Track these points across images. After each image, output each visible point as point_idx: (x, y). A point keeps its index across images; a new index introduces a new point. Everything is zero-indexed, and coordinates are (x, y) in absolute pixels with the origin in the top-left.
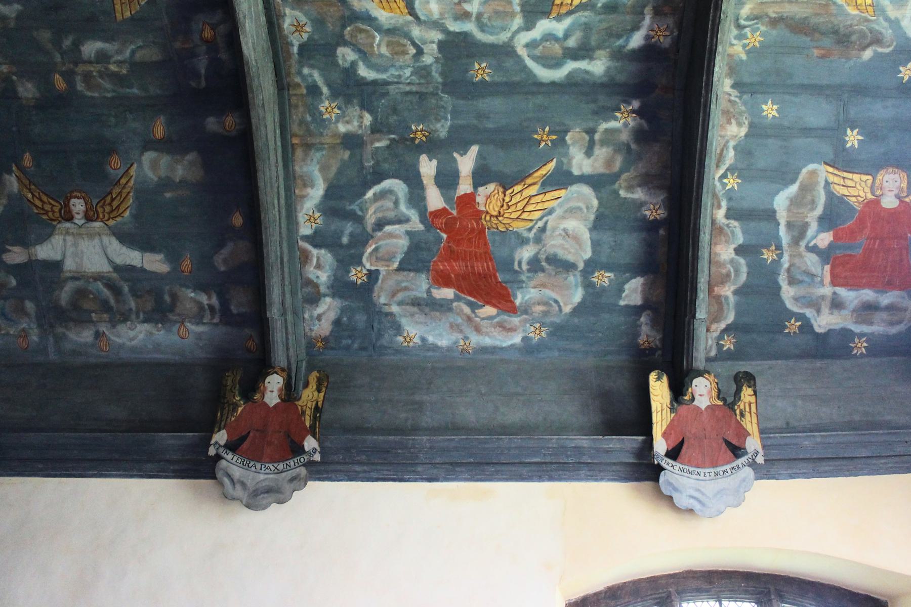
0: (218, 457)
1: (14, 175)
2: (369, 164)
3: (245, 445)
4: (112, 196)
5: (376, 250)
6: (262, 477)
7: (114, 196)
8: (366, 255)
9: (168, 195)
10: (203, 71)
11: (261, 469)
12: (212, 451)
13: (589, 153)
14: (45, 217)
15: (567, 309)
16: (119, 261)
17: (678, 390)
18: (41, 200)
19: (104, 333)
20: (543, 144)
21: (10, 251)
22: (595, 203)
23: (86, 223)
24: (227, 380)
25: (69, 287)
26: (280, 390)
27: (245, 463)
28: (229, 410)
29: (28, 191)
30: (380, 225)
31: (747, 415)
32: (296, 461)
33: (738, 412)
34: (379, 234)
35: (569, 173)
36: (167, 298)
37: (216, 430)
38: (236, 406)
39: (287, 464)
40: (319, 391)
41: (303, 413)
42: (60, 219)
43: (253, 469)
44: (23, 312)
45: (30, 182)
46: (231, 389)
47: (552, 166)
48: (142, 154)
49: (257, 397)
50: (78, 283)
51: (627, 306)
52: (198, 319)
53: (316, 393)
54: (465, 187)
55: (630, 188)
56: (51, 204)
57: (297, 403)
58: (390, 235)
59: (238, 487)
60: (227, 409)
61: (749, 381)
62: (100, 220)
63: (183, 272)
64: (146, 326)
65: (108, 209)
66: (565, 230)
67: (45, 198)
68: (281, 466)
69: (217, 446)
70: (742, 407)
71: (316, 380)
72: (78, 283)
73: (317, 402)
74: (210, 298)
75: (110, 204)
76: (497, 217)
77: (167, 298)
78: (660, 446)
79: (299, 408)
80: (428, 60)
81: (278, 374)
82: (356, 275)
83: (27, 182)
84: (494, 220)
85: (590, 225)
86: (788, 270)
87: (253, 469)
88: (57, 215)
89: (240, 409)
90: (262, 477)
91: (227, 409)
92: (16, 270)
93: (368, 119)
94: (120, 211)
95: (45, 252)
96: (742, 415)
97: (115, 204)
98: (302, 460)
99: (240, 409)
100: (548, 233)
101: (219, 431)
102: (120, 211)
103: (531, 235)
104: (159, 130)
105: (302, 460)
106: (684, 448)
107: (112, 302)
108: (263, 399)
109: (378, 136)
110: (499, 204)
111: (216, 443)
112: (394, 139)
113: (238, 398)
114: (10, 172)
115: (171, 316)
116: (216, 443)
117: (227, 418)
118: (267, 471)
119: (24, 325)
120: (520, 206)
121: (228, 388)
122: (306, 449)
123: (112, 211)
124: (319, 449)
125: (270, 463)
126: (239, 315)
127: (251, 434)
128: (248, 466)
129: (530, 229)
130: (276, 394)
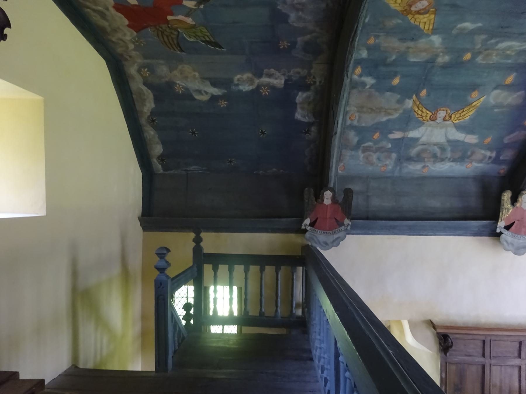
0: (501, 233)
1: (412, 100)
3: (513, 228)
4: (464, 110)
6: (521, 241)
7: (465, 110)
9: (496, 110)
14: (421, 119)
16: (451, 138)
18: (422, 111)
19: (428, 166)
21: (394, 133)
23: (442, 122)
24: (504, 197)
25: (419, 148)
28: (505, 212)
29: (417, 107)
36: (469, 153)
37: (500, 221)
38: (508, 209)
42: (429, 120)
44: (389, 157)
45: (420, 103)
49: (518, 205)
50: (424, 147)
52: (481, 161)
56: (426, 113)
59: (510, 246)
60: (505, 211)
62: (451, 120)
63: (484, 143)
64: (452, 164)
65: (458, 115)
67: (424, 110)
69: (500, 228)
72: (424, 147)
74: (492, 153)
77: (469, 153)
83: (418, 103)
88: (428, 118)
89: (510, 211)
90: (521, 241)
91: (505, 211)
92: (397, 143)
95: (412, 134)
97: (464, 113)
99: (510, 211)
101: (501, 221)
104: (510, 79)
107: (439, 154)
108: (521, 206)
111: (500, 227)
113: (509, 206)
114: (410, 98)
115: (467, 160)
117: (505, 215)
118: (524, 239)
119: (387, 163)
121: (505, 201)
123: (460, 116)
125: (524, 235)
126: (502, 160)
128: (515, 237)
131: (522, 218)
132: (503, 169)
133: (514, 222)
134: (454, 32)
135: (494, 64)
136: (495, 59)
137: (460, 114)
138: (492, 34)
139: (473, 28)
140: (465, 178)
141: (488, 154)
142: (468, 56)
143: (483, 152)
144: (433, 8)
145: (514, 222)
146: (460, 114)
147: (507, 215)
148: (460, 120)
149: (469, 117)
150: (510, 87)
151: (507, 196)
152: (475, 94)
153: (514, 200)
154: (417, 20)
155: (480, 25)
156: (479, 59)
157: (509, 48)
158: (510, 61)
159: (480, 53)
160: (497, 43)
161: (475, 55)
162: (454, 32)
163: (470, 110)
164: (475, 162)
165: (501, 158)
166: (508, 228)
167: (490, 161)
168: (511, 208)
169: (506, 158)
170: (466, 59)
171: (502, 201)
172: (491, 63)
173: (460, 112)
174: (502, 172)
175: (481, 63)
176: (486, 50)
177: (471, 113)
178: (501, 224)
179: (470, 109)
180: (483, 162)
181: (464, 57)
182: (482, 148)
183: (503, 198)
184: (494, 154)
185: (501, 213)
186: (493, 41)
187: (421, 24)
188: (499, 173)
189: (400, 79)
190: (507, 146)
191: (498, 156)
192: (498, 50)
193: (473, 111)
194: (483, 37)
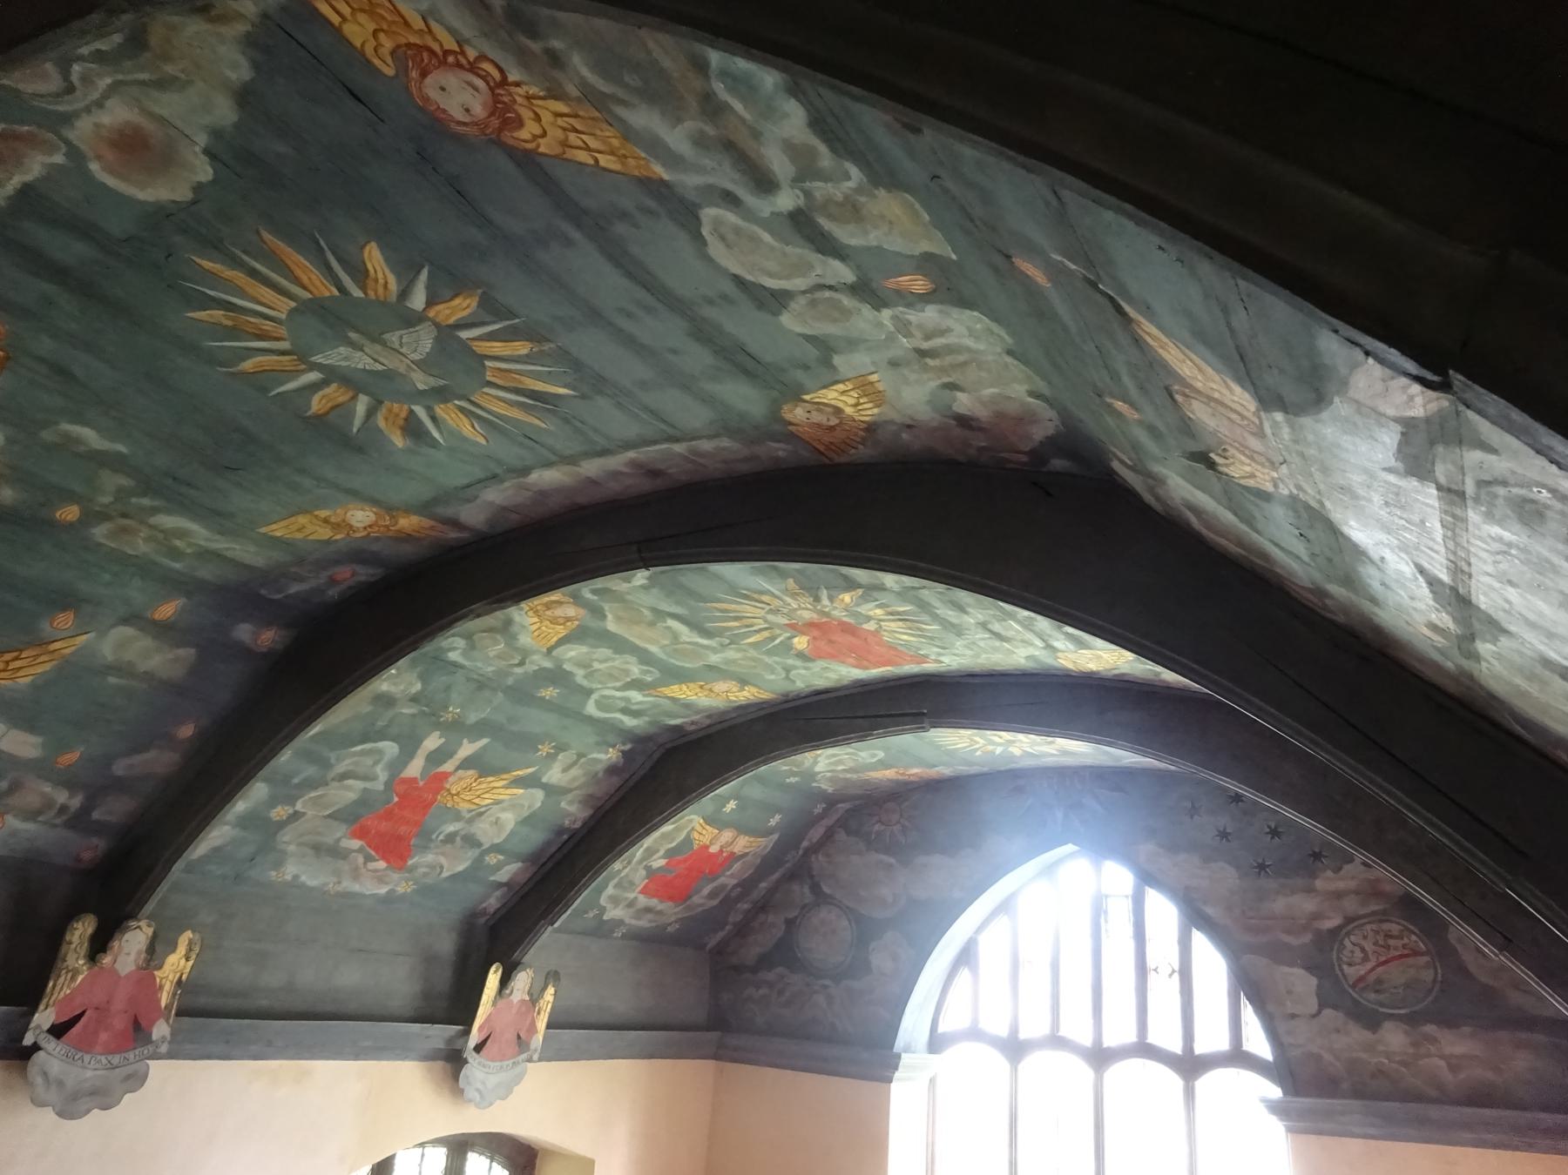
0: (36, 1047)
2: (380, 724)
4: (20, 655)
5: (320, 797)
6: (89, 1074)
8: (306, 797)
9: (112, 680)
11: (89, 1063)
12: (28, 1040)
13: (565, 770)
15: (445, 874)
17: (505, 981)
20: (540, 753)
22: (539, 804)
24: (73, 934)
26: (139, 953)
27: (70, 1054)
28: (66, 979)
30: (344, 776)
31: (542, 1013)
32: (137, 1053)
33: (537, 1008)
34: (336, 784)
35: (540, 779)
37: (42, 1007)
38: (76, 972)
39: (125, 1058)
40: (187, 959)
41: (161, 987)
43: (80, 1061)
46: (75, 949)
47: (530, 770)
48: (114, 625)
49: (107, 960)
51: (494, 881)
52: (31, 815)
53: (183, 960)
54: (448, 767)
55: (571, 803)
57: (156, 973)
58: (349, 788)
61: (555, 981)
66: (498, 819)
68: (116, 1059)
70: (541, 1005)
71: (187, 943)
73: (182, 974)
76: (453, 795)
78: (475, 1037)
79: (158, 980)
80: (518, 670)
81: (141, 929)
82: (279, 813)
84: (449, 798)
85: (519, 819)
86: (622, 878)
87: (80, 1061)
89: (80, 978)
90: (89, 1074)
91: (63, 978)
93: (418, 686)
94: (18, 675)
96: (539, 1013)
97: (18, 664)
98: (146, 1052)
99: (80, 978)
100: (483, 818)
101: (46, 1008)
102: (18, 675)
103: (468, 816)
104: (167, 610)
105: (146, 1052)
106: (489, 1041)
109: (411, 704)
110: (464, 787)
111: (38, 1026)
112: (424, 711)
113: (81, 962)
116: (38, 1026)
117: (61, 989)
118: (97, 1066)
120: (478, 793)
121: (73, 946)
122: (154, 1037)
124: (169, 1038)
125: (101, 1054)
127: (87, 1013)
129: (470, 811)
130: (132, 957)
131: (108, 1002)
132: (92, 848)
133: (83, 1013)
134: (47, 435)
135: (137, 556)
136: (140, 546)
137: (7, 663)
138: (147, 486)
139: (99, 447)
141: (62, 797)
142: (70, 513)
143: (47, 788)
145: (83, 1013)
146: (7, 663)
147: (68, 992)
149: (31, 677)
150: (164, 631)
151: (82, 930)
152: (65, 620)
153: (99, 945)
155: (121, 448)
156: (100, 532)
157: (182, 534)
158: (177, 566)
159: (103, 517)
160: (155, 511)
161: (92, 516)
162: (47, 435)
163: (38, 661)
164: (15, 816)
165: (96, 815)
166: (58, 1031)
167: (58, 821)
168: (85, 968)
169: (108, 818)
170: (63, 516)
171: (64, 948)
172: (130, 552)
173: (8, 657)
174: (87, 856)
175: (100, 545)
176: (124, 515)
177: (40, 669)
178: (44, 1017)
179: (38, 656)
180: (40, 819)
181: (60, 512)
182: (48, 779)
183: (68, 938)
184: (76, 802)
185: (51, 984)
186: (146, 502)
188: (78, 860)
190: (120, 785)
191: (85, 810)
192: (151, 527)
193: (47, 667)
194: (124, 481)
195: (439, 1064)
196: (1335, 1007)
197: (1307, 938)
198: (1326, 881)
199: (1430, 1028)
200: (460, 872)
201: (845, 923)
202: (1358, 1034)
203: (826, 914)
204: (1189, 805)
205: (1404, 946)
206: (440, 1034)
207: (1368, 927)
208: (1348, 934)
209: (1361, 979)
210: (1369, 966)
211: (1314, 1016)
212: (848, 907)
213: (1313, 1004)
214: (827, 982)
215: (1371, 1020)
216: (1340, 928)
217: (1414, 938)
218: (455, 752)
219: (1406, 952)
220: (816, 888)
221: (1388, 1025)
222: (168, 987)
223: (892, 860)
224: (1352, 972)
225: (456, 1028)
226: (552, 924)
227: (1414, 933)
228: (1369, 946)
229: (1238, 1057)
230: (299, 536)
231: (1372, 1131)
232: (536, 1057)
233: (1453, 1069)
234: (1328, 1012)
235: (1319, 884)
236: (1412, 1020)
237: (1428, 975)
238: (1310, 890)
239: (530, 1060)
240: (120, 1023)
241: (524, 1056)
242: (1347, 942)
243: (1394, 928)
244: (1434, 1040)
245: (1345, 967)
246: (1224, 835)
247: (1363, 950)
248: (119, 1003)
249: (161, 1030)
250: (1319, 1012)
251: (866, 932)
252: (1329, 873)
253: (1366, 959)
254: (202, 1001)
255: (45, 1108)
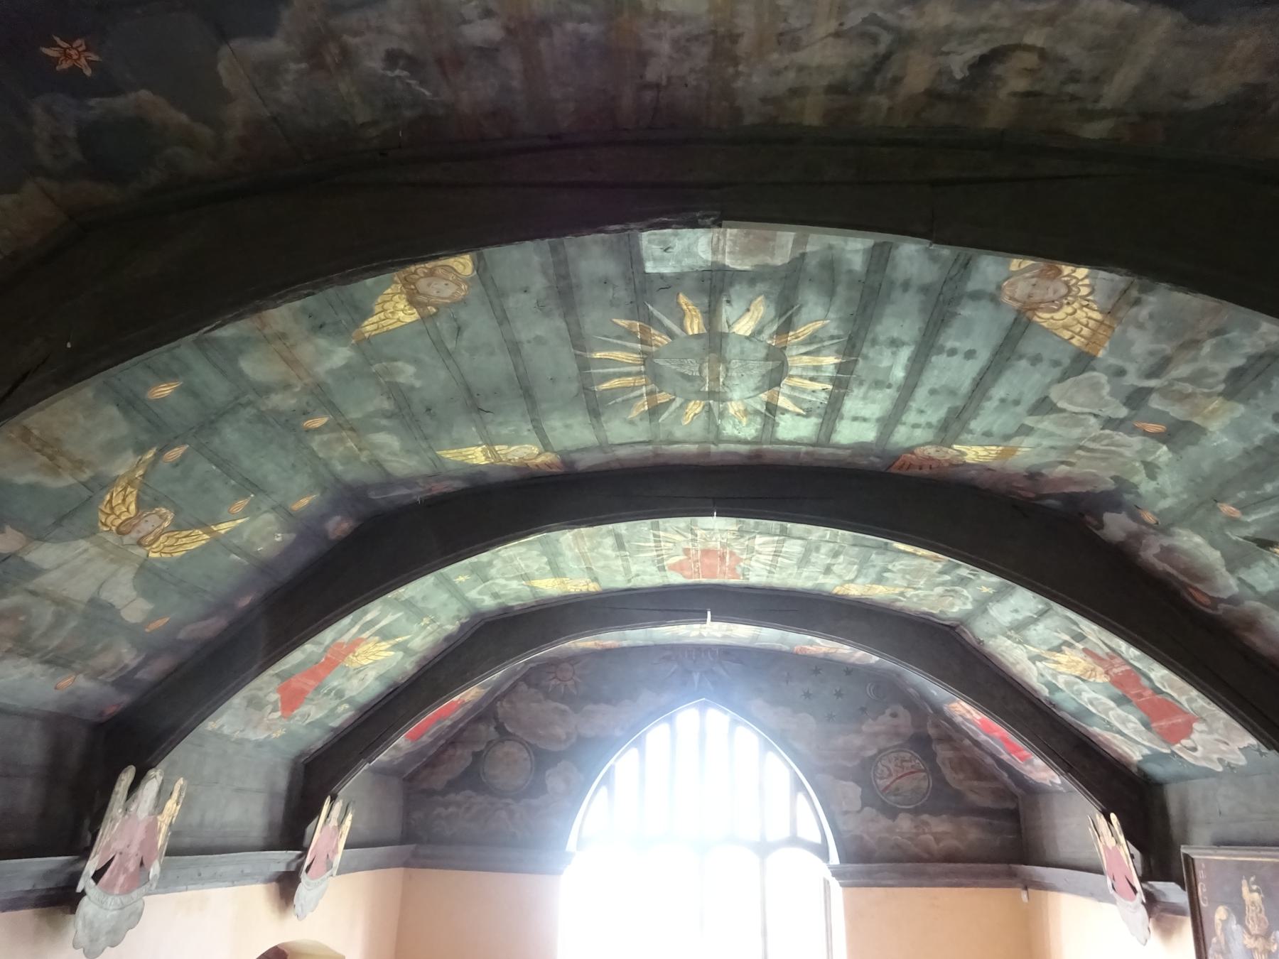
3: (106, 876)
10: (391, 495)
31: (343, 836)
40: (177, 805)
52: (95, 675)
53: (175, 805)
75: (178, 539)
131: (128, 846)
137: (178, 539)
140: (27, 715)
144: (437, 309)
148: (163, 555)
154: (387, 306)
166: (97, 876)
171: (113, 796)
178: (92, 866)
180: (100, 678)
187: (383, 313)
189: (177, 391)
195: (274, 883)
196: (872, 806)
197: (856, 762)
198: (869, 726)
199: (925, 817)
200: (317, 720)
201: (526, 755)
202: (884, 822)
203: (509, 748)
204: (786, 674)
205: (912, 767)
206: (281, 859)
207: (893, 755)
208: (881, 759)
209: (887, 788)
210: (894, 778)
211: (859, 812)
212: (527, 742)
213: (858, 804)
214: (509, 801)
215: (892, 813)
216: (875, 756)
217: (917, 761)
218: (378, 623)
219: (913, 770)
220: (500, 728)
221: (901, 815)
222: (164, 829)
223: (563, 707)
224: (883, 783)
225: (293, 854)
226: (370, 763)
227: (917, 758)
228: (892, 766)
229: (794, 841)
230: (460, 459)
231: (890, 882)
232: (335, 873)
233: (937, 840)
234: (867, 809)
235: (864, 728)
236: (916, 812)
237: (925, 784)
238: (859, 732)
239: (332, 875)
240: (132, 865)
241: (329, 873)
242: (879, 765)
243: (907, 756)
244: (926, 824)
245: (878, 781)
246: (807, 695)
247: (889, 769)
248: (134, 849)
249: (155, 870)
250: (862, 808)
251: (542, 759)
252: (870, 721)
253: (890, 775)
254: (186, 841)
255: (105, 951)
